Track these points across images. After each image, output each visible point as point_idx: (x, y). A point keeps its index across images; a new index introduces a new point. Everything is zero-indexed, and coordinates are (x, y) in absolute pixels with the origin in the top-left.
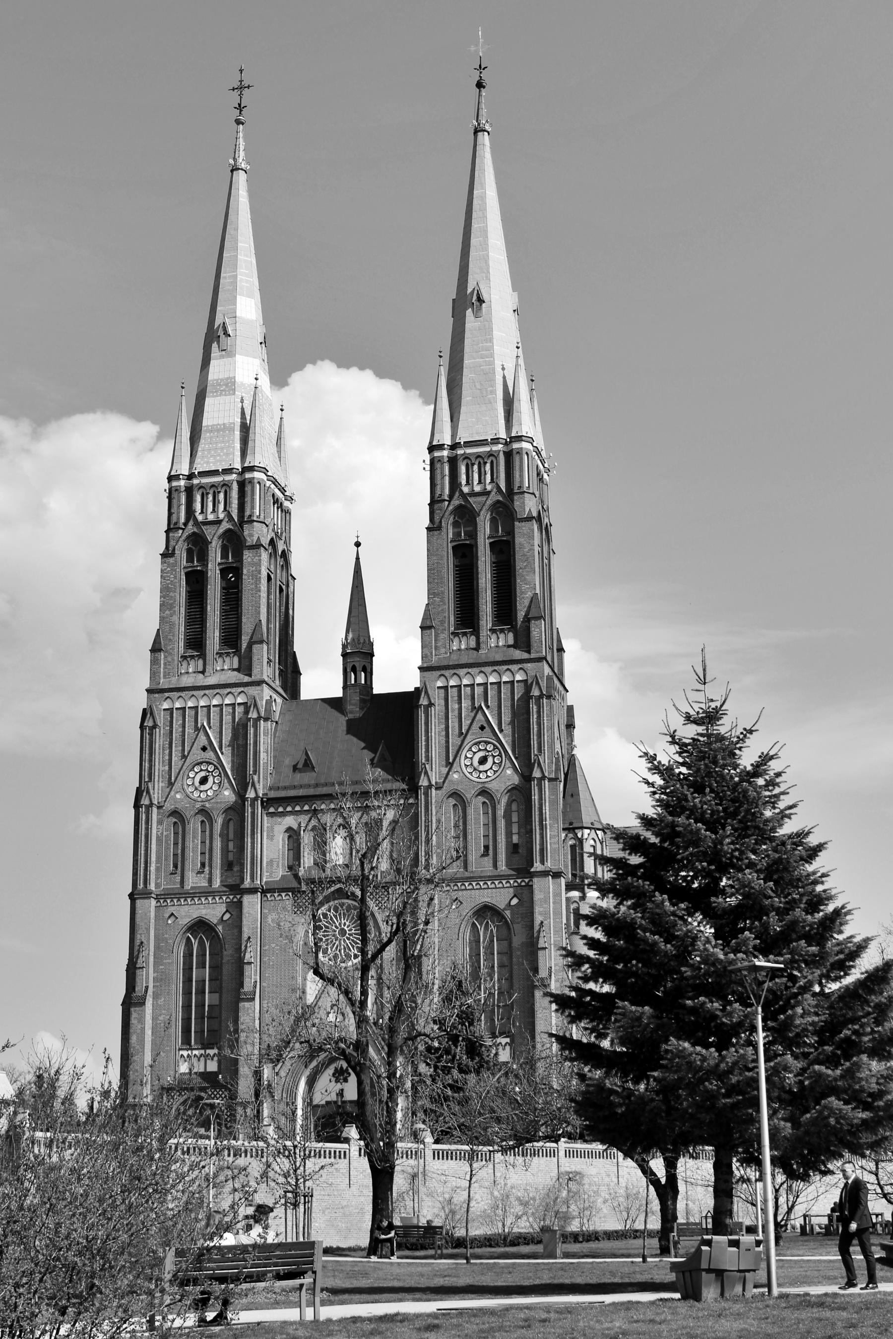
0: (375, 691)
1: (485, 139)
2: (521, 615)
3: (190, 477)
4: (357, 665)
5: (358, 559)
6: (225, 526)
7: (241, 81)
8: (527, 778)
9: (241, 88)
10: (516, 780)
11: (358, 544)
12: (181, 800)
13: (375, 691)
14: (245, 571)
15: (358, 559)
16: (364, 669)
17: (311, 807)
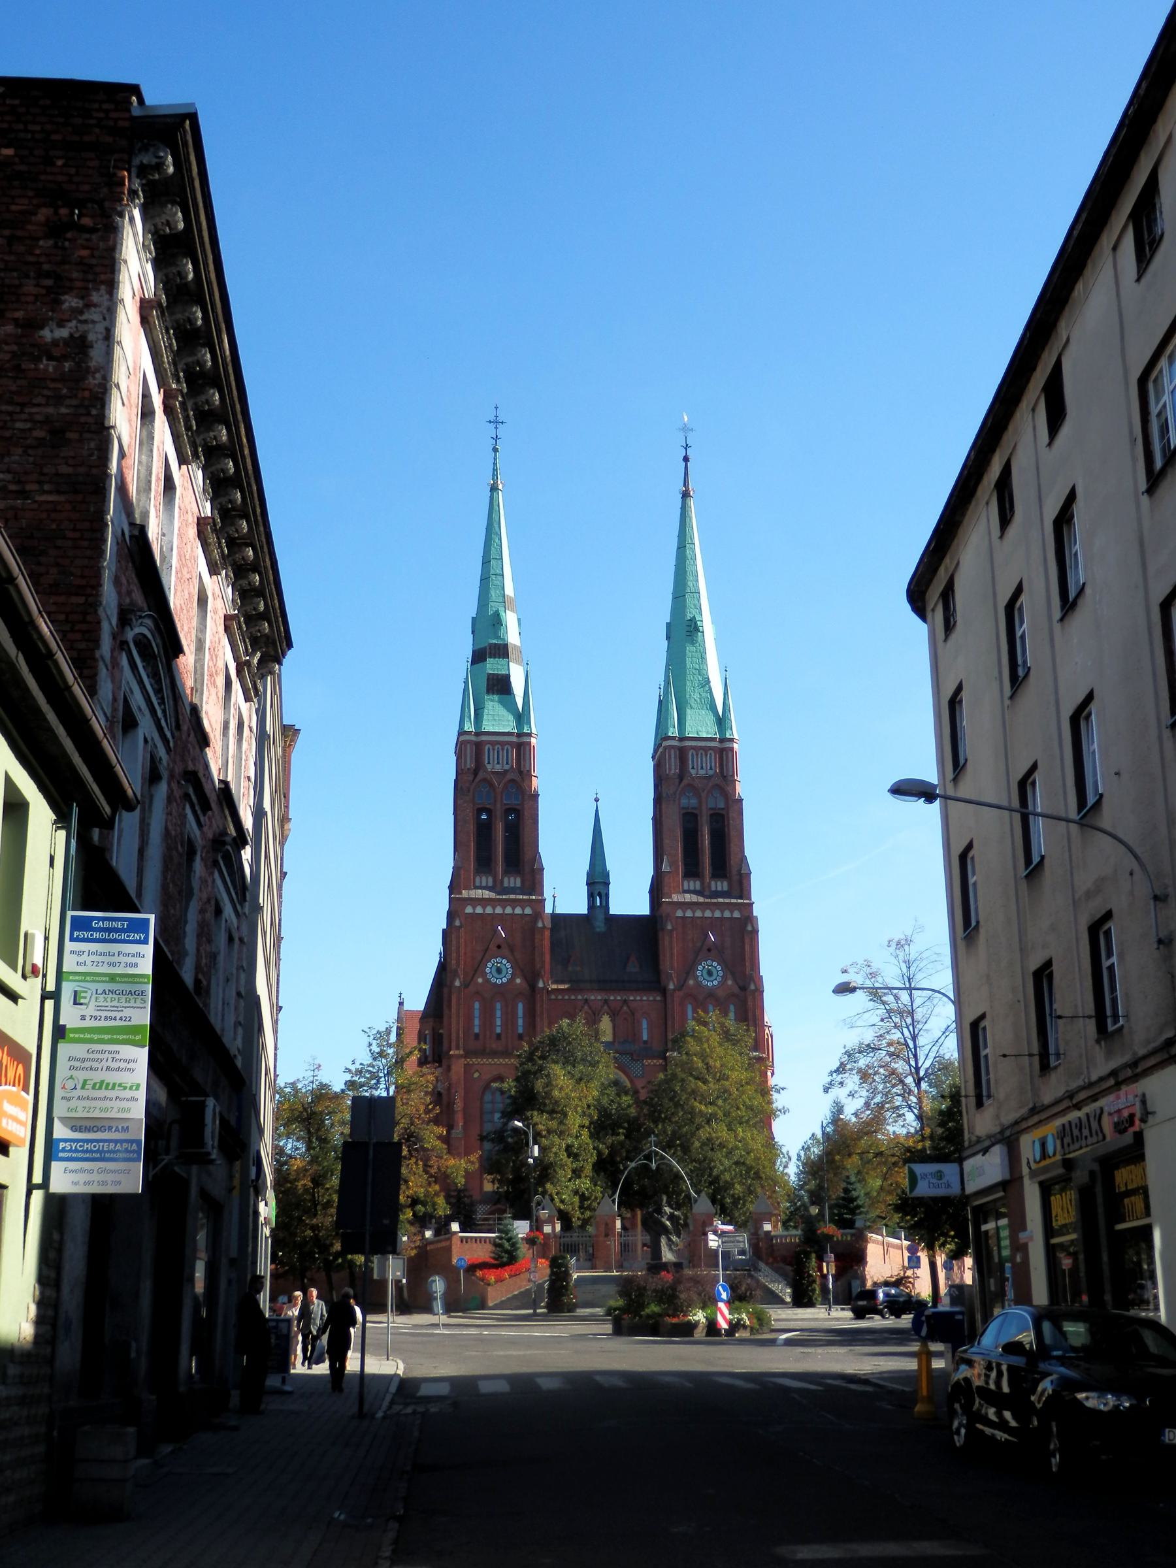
0: (611, 912)
1: (692, 503)
2: (734, 871)
3: (477, 734)
4: (602, 891)
5: (597, 811)
6: (509, 776)
7: (496, 417)
8: (744, 988)
9: (496, 422)
10: (736, 990)
11: (597, 800)
12: (481, 984)
13: (611, 912)
14: (526, 813)
15: (597, 811)
16: (600, 895)
17: (583, 997)
